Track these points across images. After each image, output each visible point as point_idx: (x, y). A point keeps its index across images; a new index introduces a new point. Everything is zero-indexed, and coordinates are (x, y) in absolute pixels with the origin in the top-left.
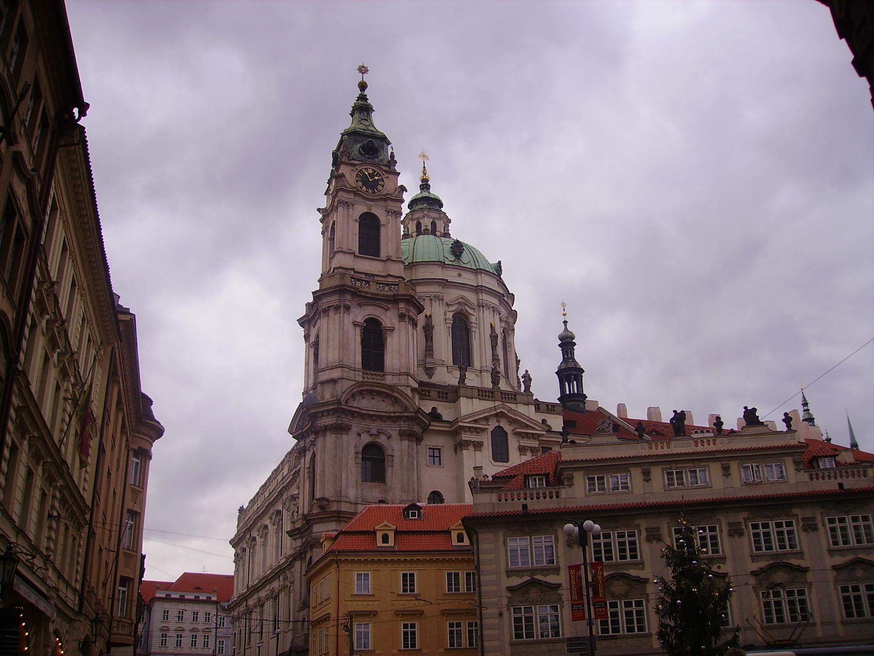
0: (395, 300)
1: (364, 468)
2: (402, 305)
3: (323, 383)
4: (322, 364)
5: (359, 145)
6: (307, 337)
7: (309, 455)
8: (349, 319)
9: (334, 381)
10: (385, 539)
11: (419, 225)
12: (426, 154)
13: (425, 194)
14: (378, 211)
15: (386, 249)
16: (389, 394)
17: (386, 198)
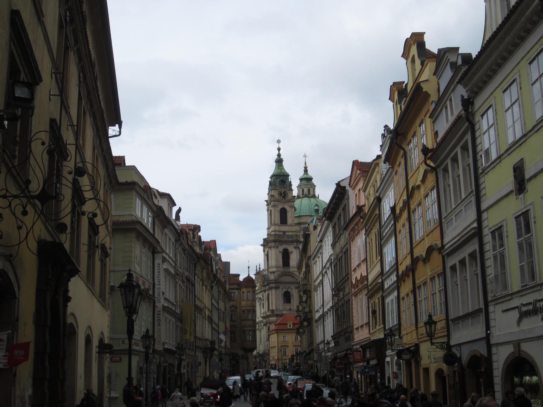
0: (292, 242)
1: (284, 299)
2: (295, 244)
3: (271, 273)
4: (270, 266)
5: (279, 180)
6: (264, 251)
7: (267, 293)
8: (278, 250)
9: (274, 272)
10: (290, 326)
11: (303, 190)
12: (307, 155)
13: (306, 176)
14: (287, 207)
15: (289, 221)
16: (291, 275)
17: (289, 201)
